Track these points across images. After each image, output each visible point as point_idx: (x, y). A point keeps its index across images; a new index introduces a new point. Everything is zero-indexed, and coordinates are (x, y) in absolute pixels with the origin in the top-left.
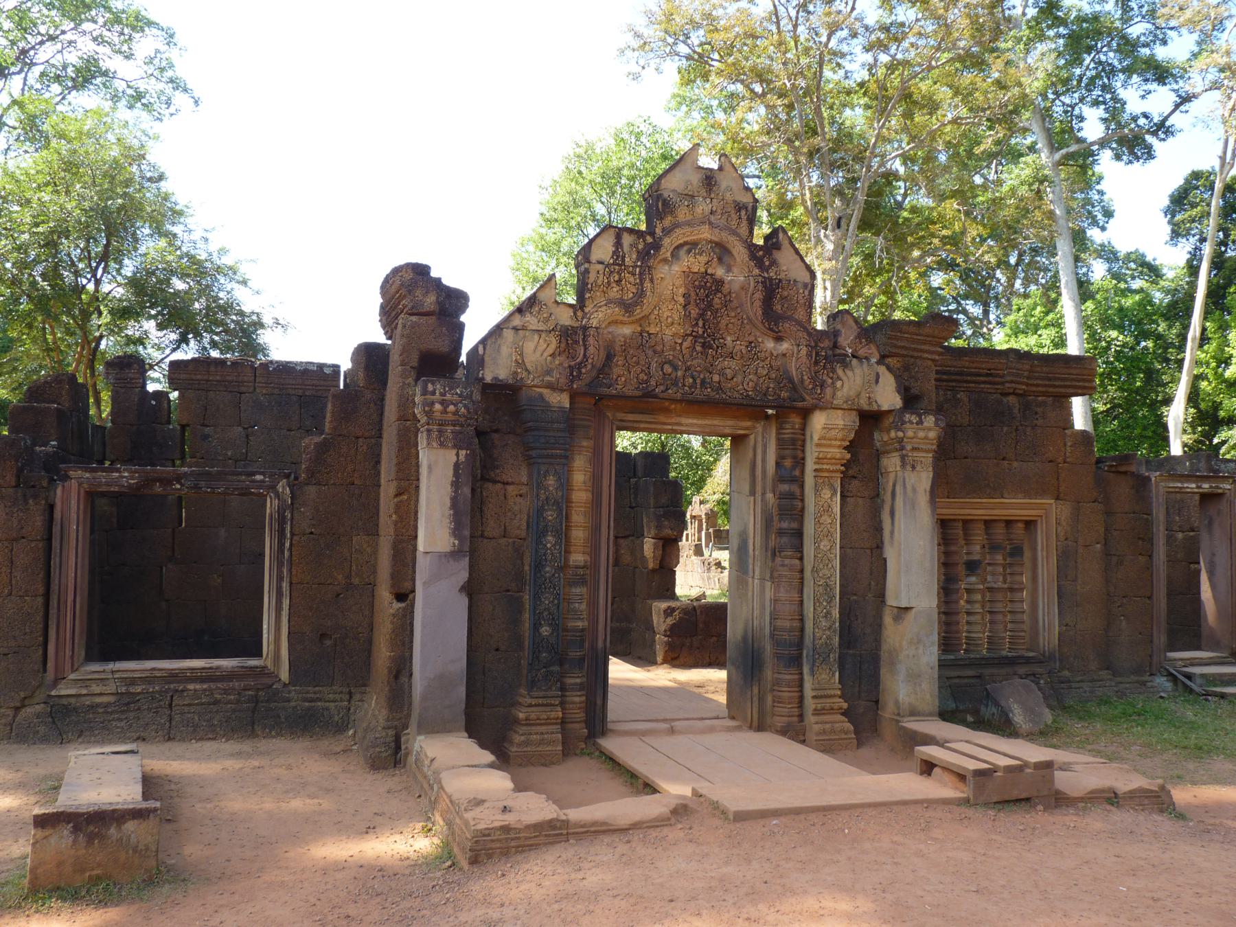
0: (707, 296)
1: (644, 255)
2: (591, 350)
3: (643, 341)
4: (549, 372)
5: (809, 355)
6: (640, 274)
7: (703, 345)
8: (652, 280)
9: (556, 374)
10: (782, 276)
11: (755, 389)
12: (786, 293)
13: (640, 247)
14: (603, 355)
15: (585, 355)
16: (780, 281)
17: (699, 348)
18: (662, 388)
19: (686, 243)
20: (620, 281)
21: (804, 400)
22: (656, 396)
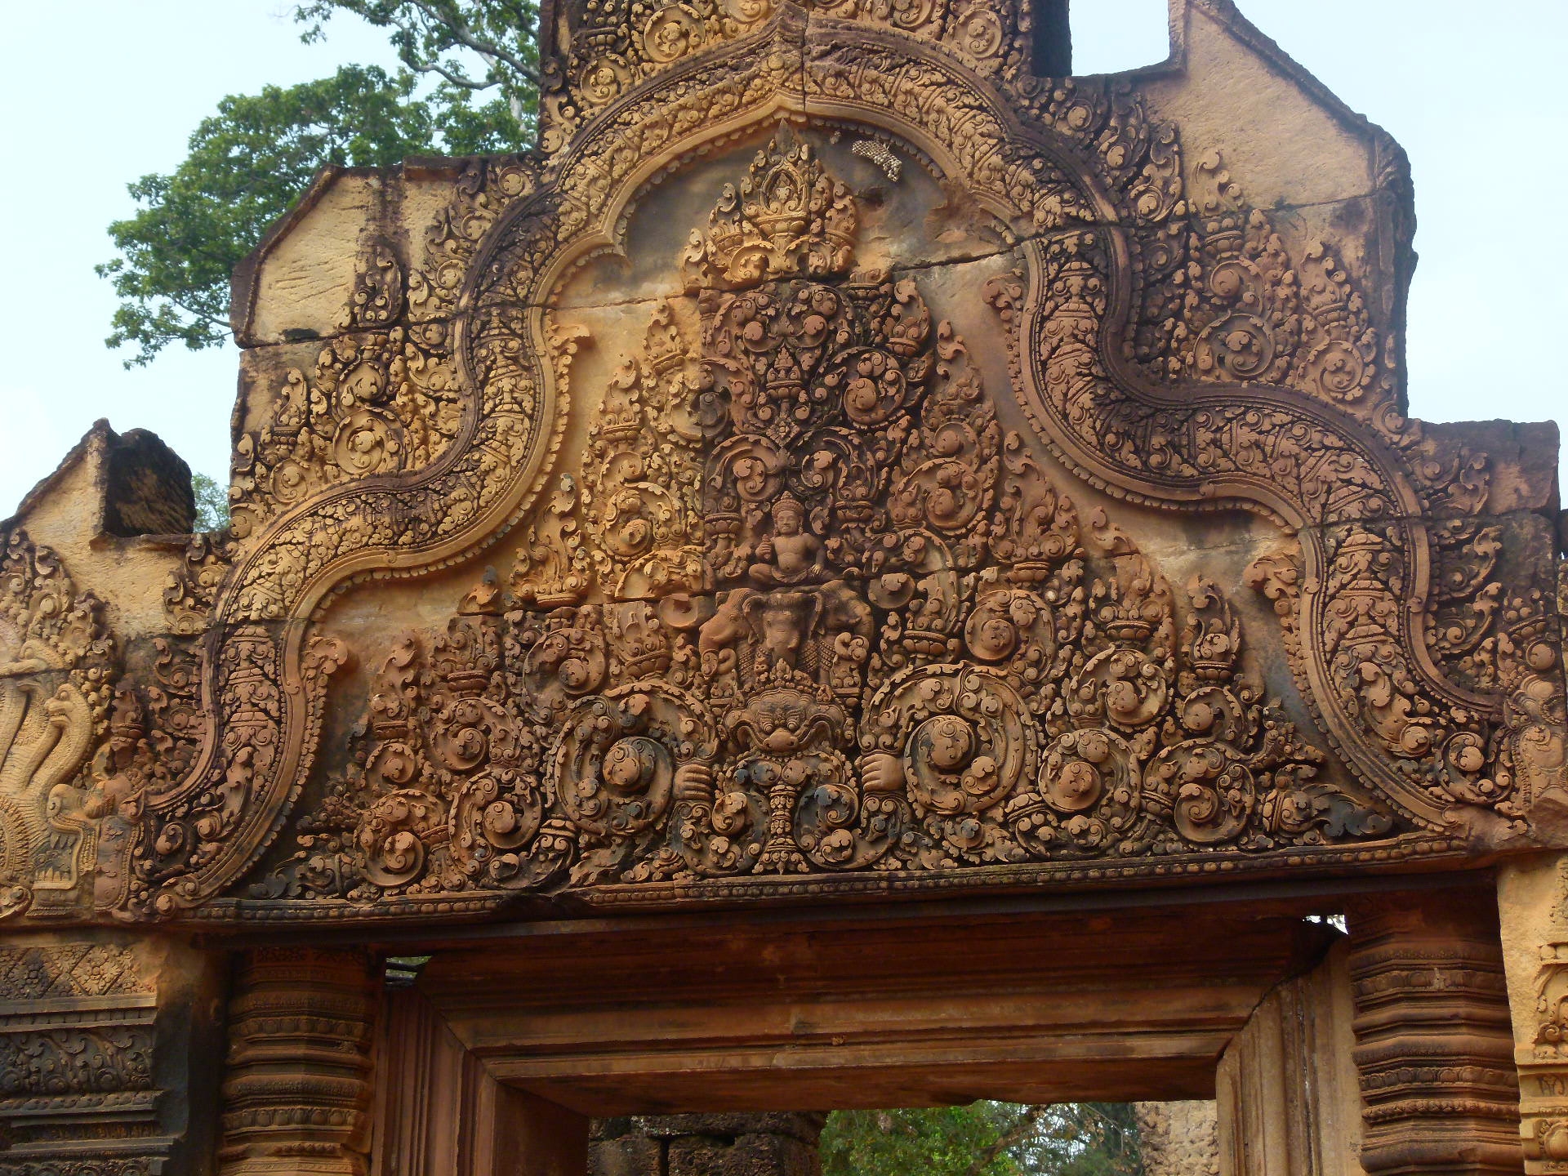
0: (810, 378)
1: (491, 262)
2: (244, 722)
3: (521, 653)
4: (49, 857)
5: (1390, 568)
6: (472, 341)
7: (805, 620)
8: (522, 362)
9: (80, 860)
10: (1203, 194)
11: (1090, 802)
12: (1223, 280)
13: (476, 229)
14: (304, 736)
15: (218, 752)
16: (1190, 220)
17: (777, 634)
18: (604, 858)
19: (693, 163)
20: (380, 400)
21: (1401, 824)
22: (574, 907)
